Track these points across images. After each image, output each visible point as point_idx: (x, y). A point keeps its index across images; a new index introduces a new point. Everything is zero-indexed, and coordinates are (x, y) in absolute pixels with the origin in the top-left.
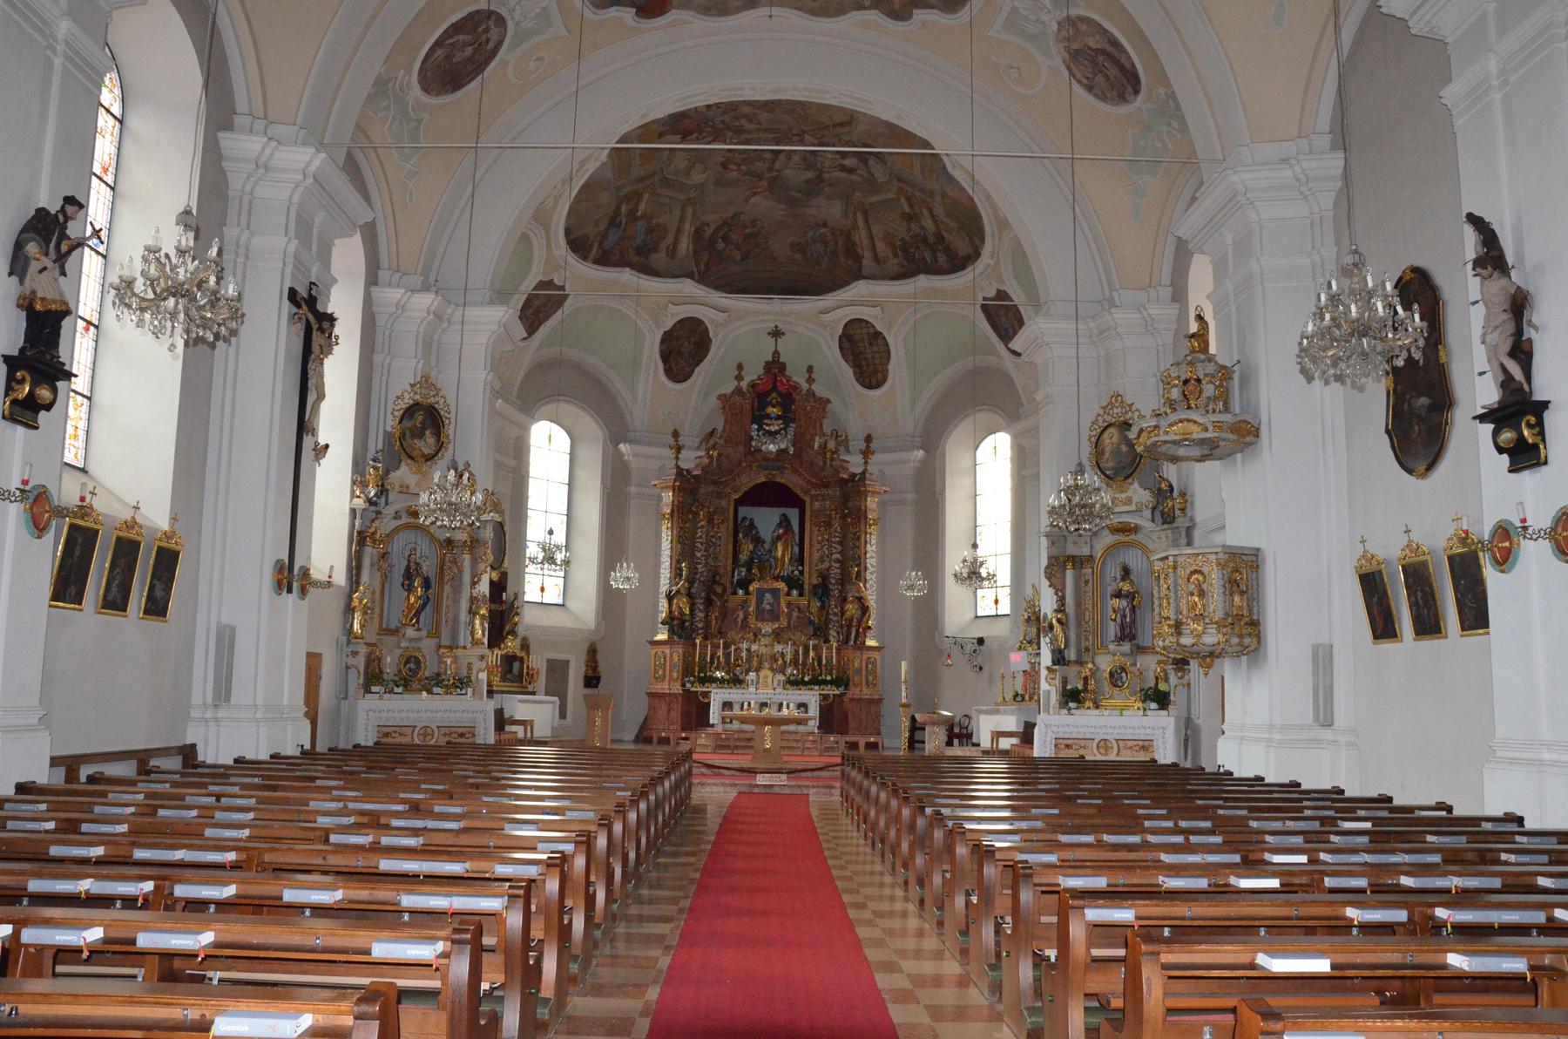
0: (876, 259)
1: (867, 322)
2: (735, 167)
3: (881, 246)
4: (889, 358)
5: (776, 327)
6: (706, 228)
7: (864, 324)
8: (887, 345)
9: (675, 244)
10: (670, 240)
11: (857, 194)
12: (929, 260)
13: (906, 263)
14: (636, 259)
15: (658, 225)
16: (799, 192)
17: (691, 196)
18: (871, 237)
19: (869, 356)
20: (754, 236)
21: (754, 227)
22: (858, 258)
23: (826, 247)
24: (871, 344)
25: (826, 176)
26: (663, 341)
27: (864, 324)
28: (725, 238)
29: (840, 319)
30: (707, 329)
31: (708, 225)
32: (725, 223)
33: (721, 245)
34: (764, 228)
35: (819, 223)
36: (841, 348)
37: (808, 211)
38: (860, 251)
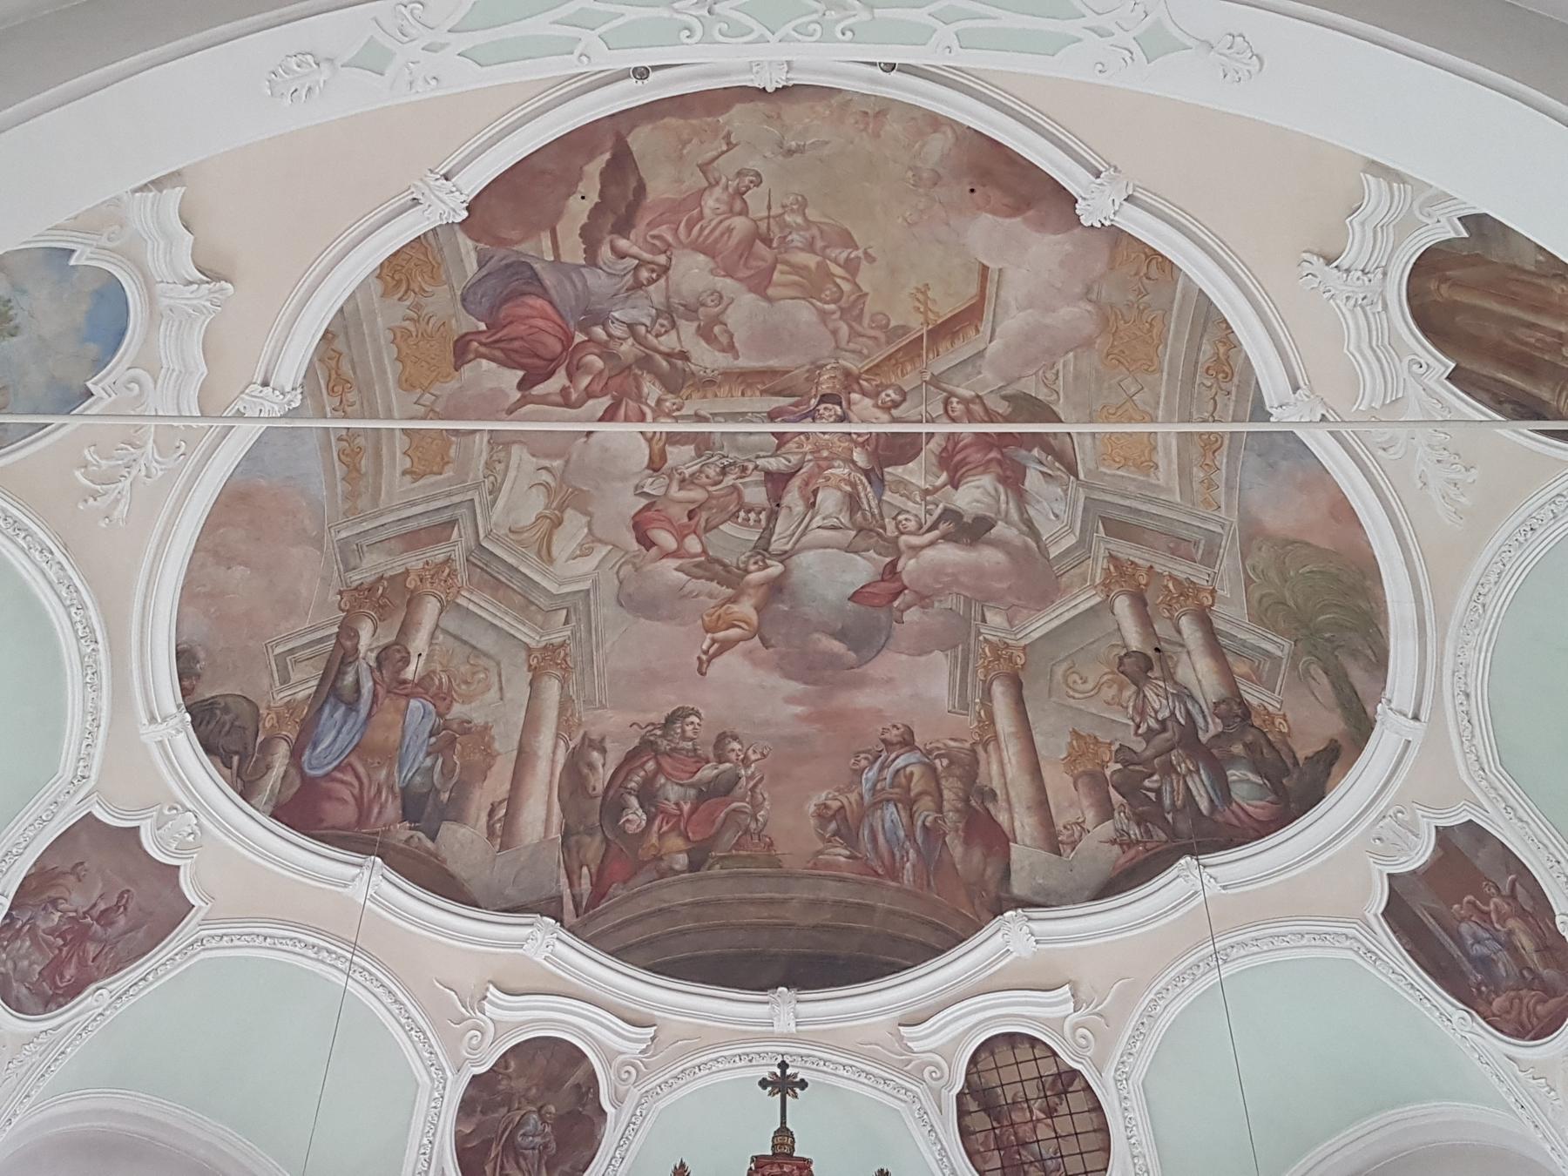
0: (1053, 843)
1: (1033, 1041)
2: (666, 540)
3: (1057, 780)
4: (1107, 1149)
5: (783, 1066)
6: (595, 755)
7: (1024, 1052)
8: (1098, 1108)
9: (514, 799)
10: (496, 785)
11: (995, 619)
12: (1204, 805)
13: (1135, 832)
14: (402, 832)
15: (465, 727)
16: (840, 635)
17: (557, 638)
18: (1035, 771)
19: (1048, 1150)
20: (722, 789)
21: (721, 760)
22: (996, 840)
23: (911, 817)
24: (1050, 1112)
25: (908, 565)
26: (467, 1107)
27: (1024, 1052)
28: (648, 796)
29: (958, 1040)
30: (593, 1076)
31: (603, 751)
32: (646, 747)
33: (635, 816)
34: (746, 762)
35: (893, 735)
36: (964, 1133)
37: (863, 699)
38: (1002, 818)
